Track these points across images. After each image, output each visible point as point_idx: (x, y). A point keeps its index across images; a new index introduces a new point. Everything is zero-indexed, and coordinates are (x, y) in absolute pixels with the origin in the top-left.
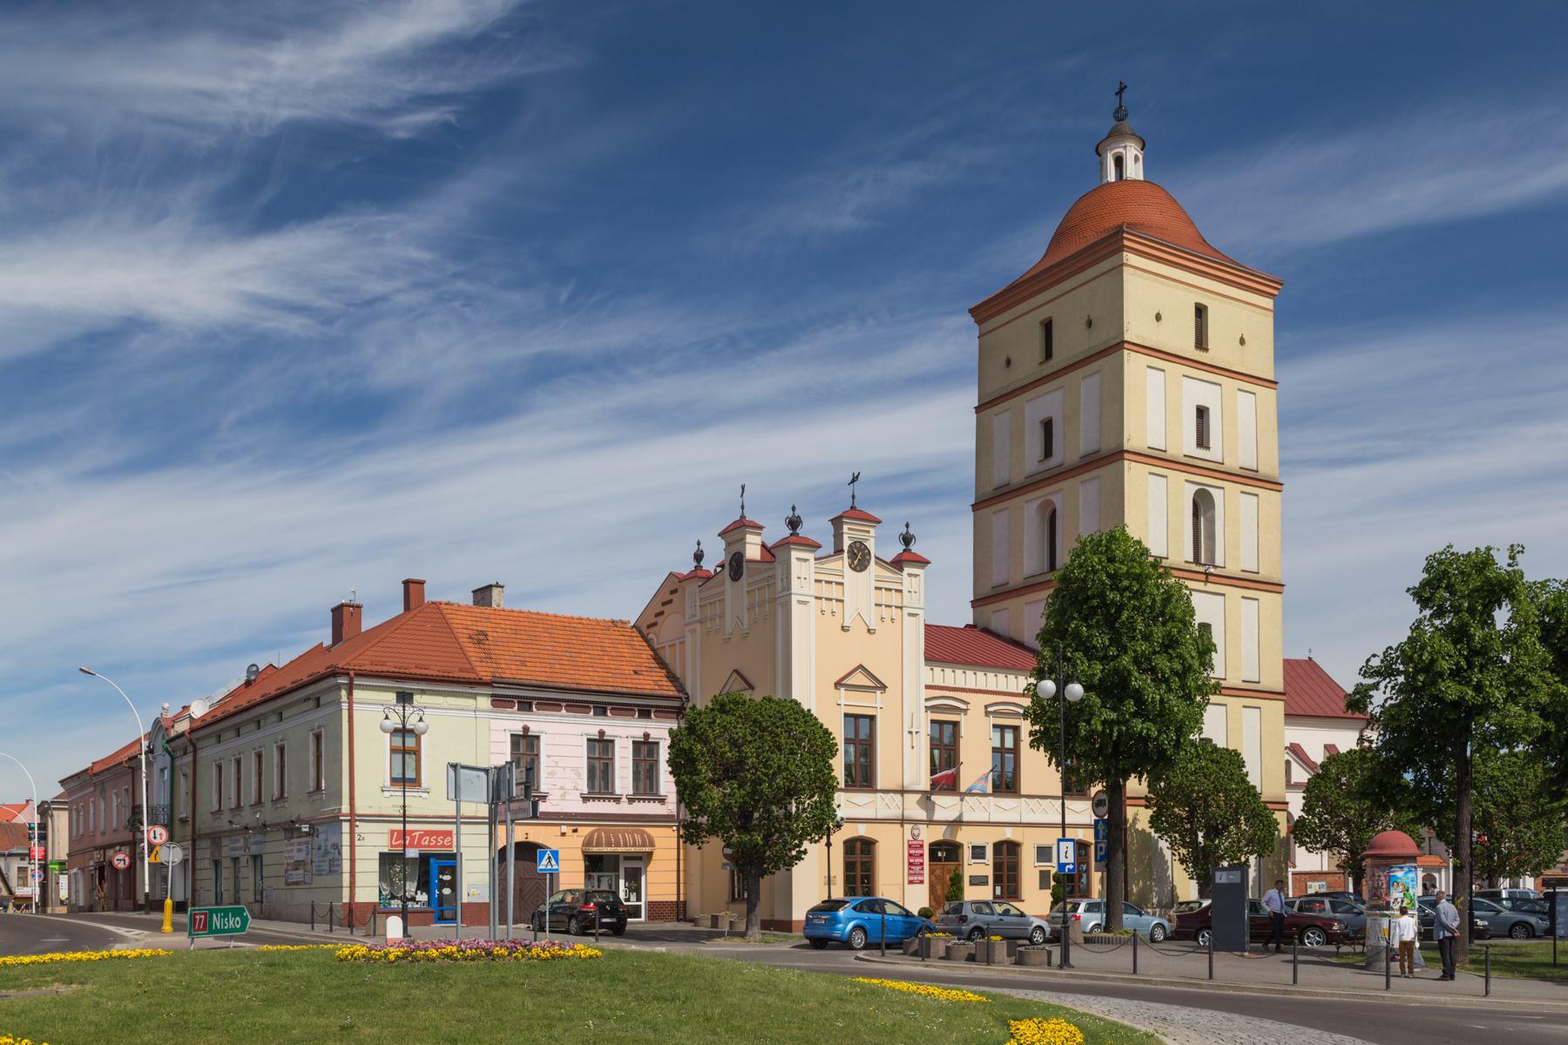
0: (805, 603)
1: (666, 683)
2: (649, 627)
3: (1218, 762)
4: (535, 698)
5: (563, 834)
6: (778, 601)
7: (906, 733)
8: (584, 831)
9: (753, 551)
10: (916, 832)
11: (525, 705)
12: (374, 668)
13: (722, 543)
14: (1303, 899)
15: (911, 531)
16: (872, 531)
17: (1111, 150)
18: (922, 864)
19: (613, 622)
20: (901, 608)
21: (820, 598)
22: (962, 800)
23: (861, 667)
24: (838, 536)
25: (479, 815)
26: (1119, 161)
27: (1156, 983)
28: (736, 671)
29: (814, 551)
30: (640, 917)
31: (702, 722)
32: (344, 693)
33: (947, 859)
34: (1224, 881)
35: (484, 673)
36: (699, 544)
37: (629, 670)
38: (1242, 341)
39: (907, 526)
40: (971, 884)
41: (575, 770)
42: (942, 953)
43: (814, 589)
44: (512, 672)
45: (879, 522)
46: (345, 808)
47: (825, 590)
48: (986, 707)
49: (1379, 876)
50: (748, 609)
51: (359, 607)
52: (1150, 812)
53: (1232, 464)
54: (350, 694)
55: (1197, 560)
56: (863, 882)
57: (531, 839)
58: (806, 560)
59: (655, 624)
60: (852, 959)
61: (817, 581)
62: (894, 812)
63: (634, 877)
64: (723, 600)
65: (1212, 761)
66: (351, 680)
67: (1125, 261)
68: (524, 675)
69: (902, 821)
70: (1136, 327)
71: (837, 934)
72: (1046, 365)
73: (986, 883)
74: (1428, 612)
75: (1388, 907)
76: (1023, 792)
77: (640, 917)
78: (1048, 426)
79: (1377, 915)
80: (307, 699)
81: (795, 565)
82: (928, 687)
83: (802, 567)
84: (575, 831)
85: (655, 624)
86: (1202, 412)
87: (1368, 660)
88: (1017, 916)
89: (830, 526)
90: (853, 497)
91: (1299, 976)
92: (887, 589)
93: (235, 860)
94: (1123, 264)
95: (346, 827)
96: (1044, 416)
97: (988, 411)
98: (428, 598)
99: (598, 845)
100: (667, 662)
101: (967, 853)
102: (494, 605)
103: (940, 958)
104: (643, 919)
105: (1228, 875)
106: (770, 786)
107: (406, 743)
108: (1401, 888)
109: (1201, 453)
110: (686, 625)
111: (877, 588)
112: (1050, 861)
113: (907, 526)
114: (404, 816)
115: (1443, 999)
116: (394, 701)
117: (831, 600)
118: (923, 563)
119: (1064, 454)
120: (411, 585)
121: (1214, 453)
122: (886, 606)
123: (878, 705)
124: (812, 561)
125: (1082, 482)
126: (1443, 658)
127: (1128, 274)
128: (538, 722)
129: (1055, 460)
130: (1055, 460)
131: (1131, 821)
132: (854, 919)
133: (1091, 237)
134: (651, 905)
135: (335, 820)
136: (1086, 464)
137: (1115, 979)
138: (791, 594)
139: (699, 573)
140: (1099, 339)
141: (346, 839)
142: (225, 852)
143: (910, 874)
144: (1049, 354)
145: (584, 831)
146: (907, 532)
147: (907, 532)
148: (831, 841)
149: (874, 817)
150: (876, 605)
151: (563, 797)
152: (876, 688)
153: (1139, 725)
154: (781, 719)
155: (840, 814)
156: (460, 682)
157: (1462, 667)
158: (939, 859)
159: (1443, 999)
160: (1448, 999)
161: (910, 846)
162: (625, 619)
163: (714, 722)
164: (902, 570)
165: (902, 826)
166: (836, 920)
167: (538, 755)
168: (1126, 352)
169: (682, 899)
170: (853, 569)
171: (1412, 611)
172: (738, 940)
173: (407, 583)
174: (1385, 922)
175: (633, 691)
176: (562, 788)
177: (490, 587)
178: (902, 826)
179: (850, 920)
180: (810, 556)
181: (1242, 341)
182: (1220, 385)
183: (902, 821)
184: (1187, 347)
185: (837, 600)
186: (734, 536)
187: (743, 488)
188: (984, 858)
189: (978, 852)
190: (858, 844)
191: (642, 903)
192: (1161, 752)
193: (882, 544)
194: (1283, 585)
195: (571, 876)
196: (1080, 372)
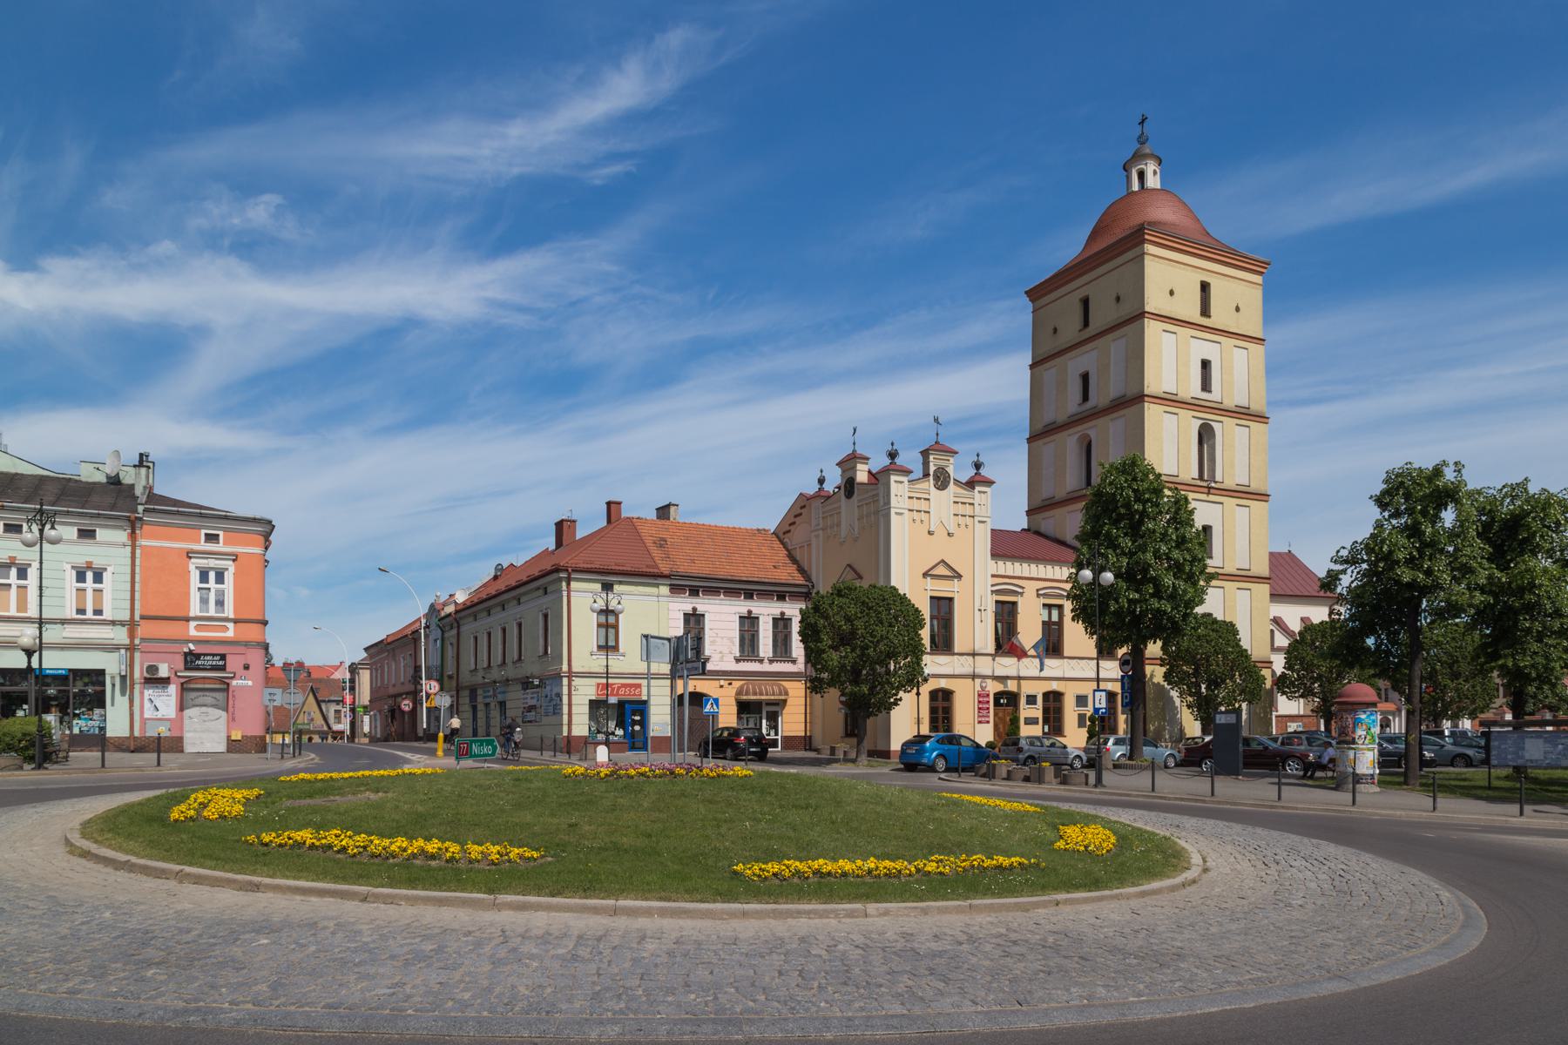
0: (901, 514)
1: (797, 574)
2: (784, 533)
3: (1217, 631)
4: (701, 587)
5: (722, 686)
6: (881, 513)
7: (977, 612)
8: (737, 684)
9: (862, 476)
10: (984, 685)
11: (694, 592)
12: (586, 566)
13: (839, 471)
14: (1285, 736)
15: (981, 459)
16: (952, 460)
17: (1136, 166)
18: (988, 708)
19: (758, 530)
20: (973, 517)
21: (912, 510)
23: (943, 561)
24: (926, 464)
25: (661, 672)
26: (1141, 175)
27: (1170, 799)
28: (849, 565)
29: (907, 476)
30: (777, 747)
31: (824, 603)
32: (564, 584)
33: (1007, 705)
34: (1223, 721)
35: (664, 568)
36: (821, 471)
37: (769, 565)
38: (1238, 309)
39: (978, 455)
40: (1026, 724)
41: (731, 639)
42: (1005, 775)
43: (907, 504)
44: (684, 568)
45: (957, 453)
46: (565, 667)
47: (916, 505)
48: (1038, 590)
49: (1347, 718)
50: (858, 519)
51: (574, 521)
52: (1164, 669)
53: (1229, 403)
54: (568, 585)
55: (1201, 477)
56: (944, 722)
57: (698, 690)
58: (901, 482)
59: (789, 531)
60: (936, 779)
61: (910, 498)
62: (968, 670)
63: (773, 719)
64: (840, 513)
65: (1213, 630)
66: (569, 574)
67: (1146, 251)
68: (694, 570)
69: (974, 677)
70: (1155, 300)
71: (925, 761)
72: (1082, 333)
73: (1037, 723)
74: (1386, 514)
75: (1353, 742)
76: (1065, 655)
77: (777, 747)
78: (1085, 378)
79: (1345, 748)
80: (538, 588)
81: (893, 486)
82: (993, 576)
83: (899, 489)
84: (730, 684)
85: (789, 531)
86: (1206, 365)
87: (1338, 552)
88: (1061, 747)
89: (920, 458)
90: (937, 434)
91: (1283, 795)
92: (962, 503)
93: (487, 705)
94: (1144, 253)
95: (565, 681)
96: (1082, 370)
97: (1039, 367)
98: (624, 514)
99: (747, 694)
100: (798, 559)
101: (1023, 700)
102: (671, 519)
103: (1004, 779)
104: (779, 749)
105: (1226, 718)
106: (875, 651)
107: (608, 620)
108: (1364, 727)
109: (1205, 395)
110: (812, 532)
111: (955, 502)
112: (1086, 706)
113: (978, 455)
114: (607, 673)
115: (1398, 813)
116: (600, 590)
117: (920, 511)
118: (989, 483)
119: (1098, 399)
120: (612, 505)
121: (1215, 395)
122: (962, 515)
123: (956, 590)
124: (906, 482)
125: (1112, 420)
126: (1399, 550)
127: (1148, 260)
128: (704, 605)
129: (1090, 404)
130: (1090, 404)
131: (1149, 676)
132: (938, 749)
133: (1118, 233)
134: (785, 738)
135: (558, 677)
136: (1116, 406)
137: (1138, 796)
138: (890, 508)
139: (823, 493)
140: (1126, 310)
141: (565, 690)
142: (480, 699)
143: (979, 716)
144: (1086, 324)
145: (737, 684)
146: (978, 460)
147: (978, 460)
148: (920, 691)
150: (955, 515)
151: (721, 659)
152: (954, 577)
153: (1154, 603)
154: (883, 601)
155: (927, 671)
156: (647, 576)
157: (1414, 556)
158: (1002, 705)
159: (1398, 813)
160: (1403, 813)
161: (979, 695)
162: (767, 528)
163: (833, 603)
164: (974, 488)
165: (973, 679)
166: (924, 750)
167: (703, 628)
168: (1146, 320)
169: (808, 734)
170: (938, 489)
171: (1375, 513)
172: (850, 765)
173: (609, 504)
174: (1351, 753)
175: (773, 581)
176: (721, 653)
177: (668, 506)
178: (973, 679)
179: (934, 750)
180: (905, 479)
181: (1238, 309)
182: (1220, 343)
183: (974, 677)
184: (1193, 314)
185: (925, 512)
186: (848, 465)
187: (855, 430)
188: (1035, 704)
189: (1031, 700)
191: (779, 737)
192: (1174, 623)
193: (959, 469)
194: (1269, 495)
195: (728, 717)
196: (1110, 336)
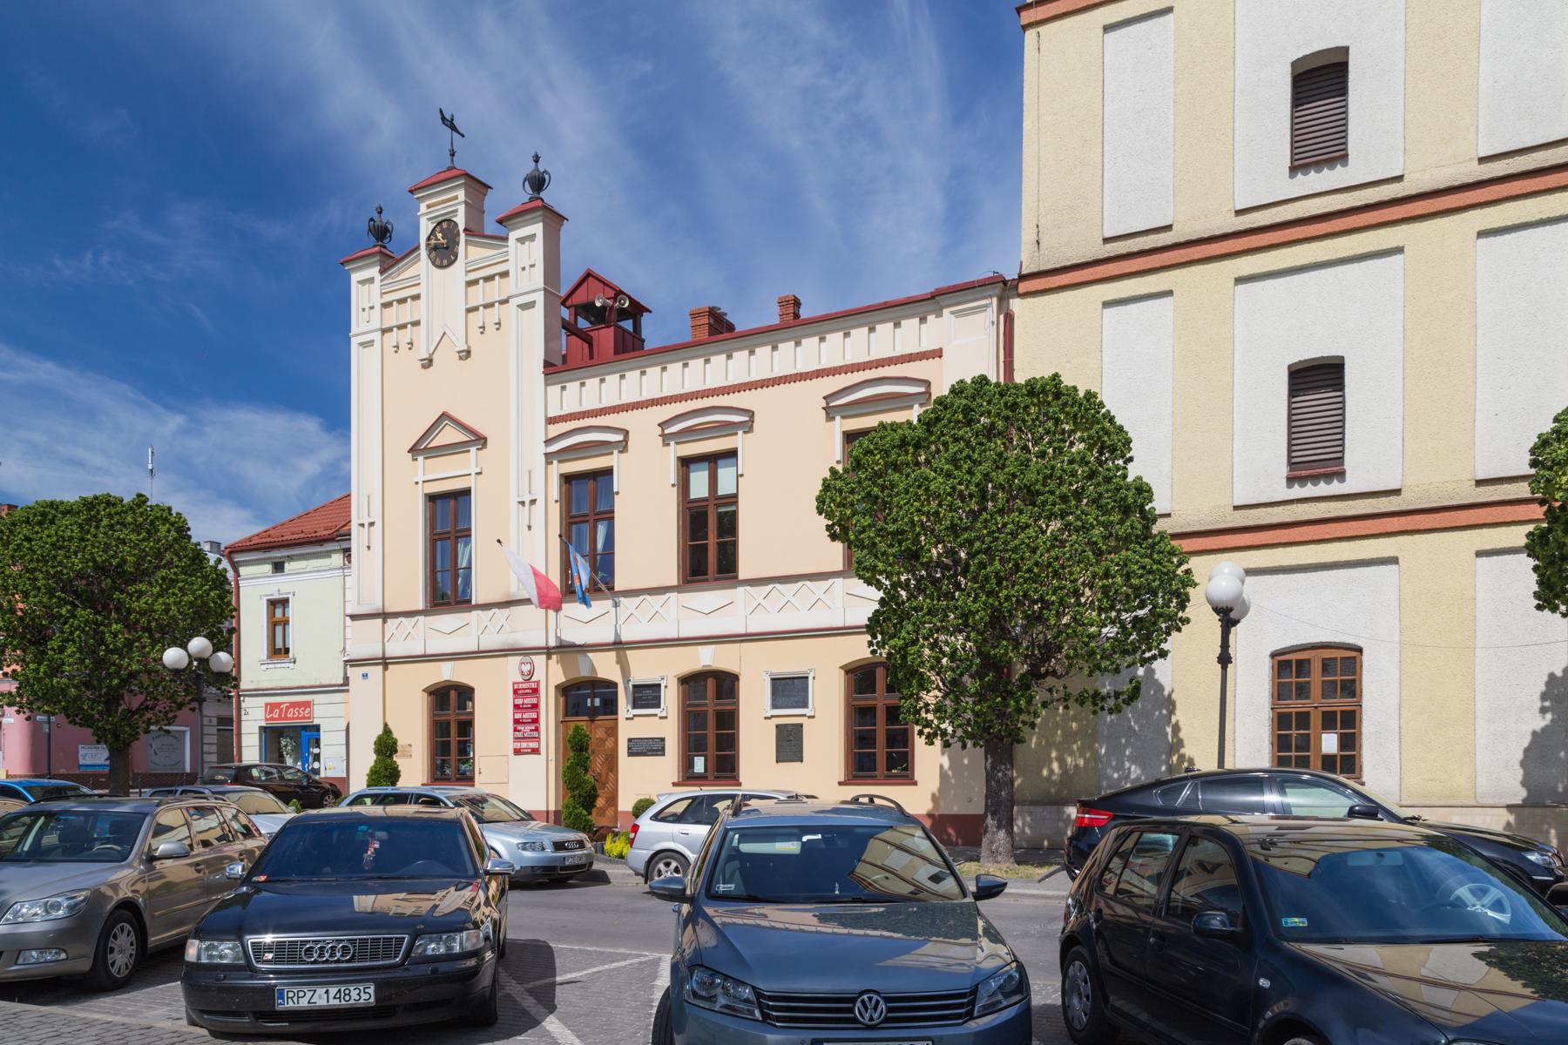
22: (616, 605)
40: (631, 754)
73: (660, 751)
82: (551, 421)
143: (516, 739)
146: (537, 169)
149: (676, 636)
161: (515, 691)
188: (874, 692)
189: (647, 696)
190: (453, 694)
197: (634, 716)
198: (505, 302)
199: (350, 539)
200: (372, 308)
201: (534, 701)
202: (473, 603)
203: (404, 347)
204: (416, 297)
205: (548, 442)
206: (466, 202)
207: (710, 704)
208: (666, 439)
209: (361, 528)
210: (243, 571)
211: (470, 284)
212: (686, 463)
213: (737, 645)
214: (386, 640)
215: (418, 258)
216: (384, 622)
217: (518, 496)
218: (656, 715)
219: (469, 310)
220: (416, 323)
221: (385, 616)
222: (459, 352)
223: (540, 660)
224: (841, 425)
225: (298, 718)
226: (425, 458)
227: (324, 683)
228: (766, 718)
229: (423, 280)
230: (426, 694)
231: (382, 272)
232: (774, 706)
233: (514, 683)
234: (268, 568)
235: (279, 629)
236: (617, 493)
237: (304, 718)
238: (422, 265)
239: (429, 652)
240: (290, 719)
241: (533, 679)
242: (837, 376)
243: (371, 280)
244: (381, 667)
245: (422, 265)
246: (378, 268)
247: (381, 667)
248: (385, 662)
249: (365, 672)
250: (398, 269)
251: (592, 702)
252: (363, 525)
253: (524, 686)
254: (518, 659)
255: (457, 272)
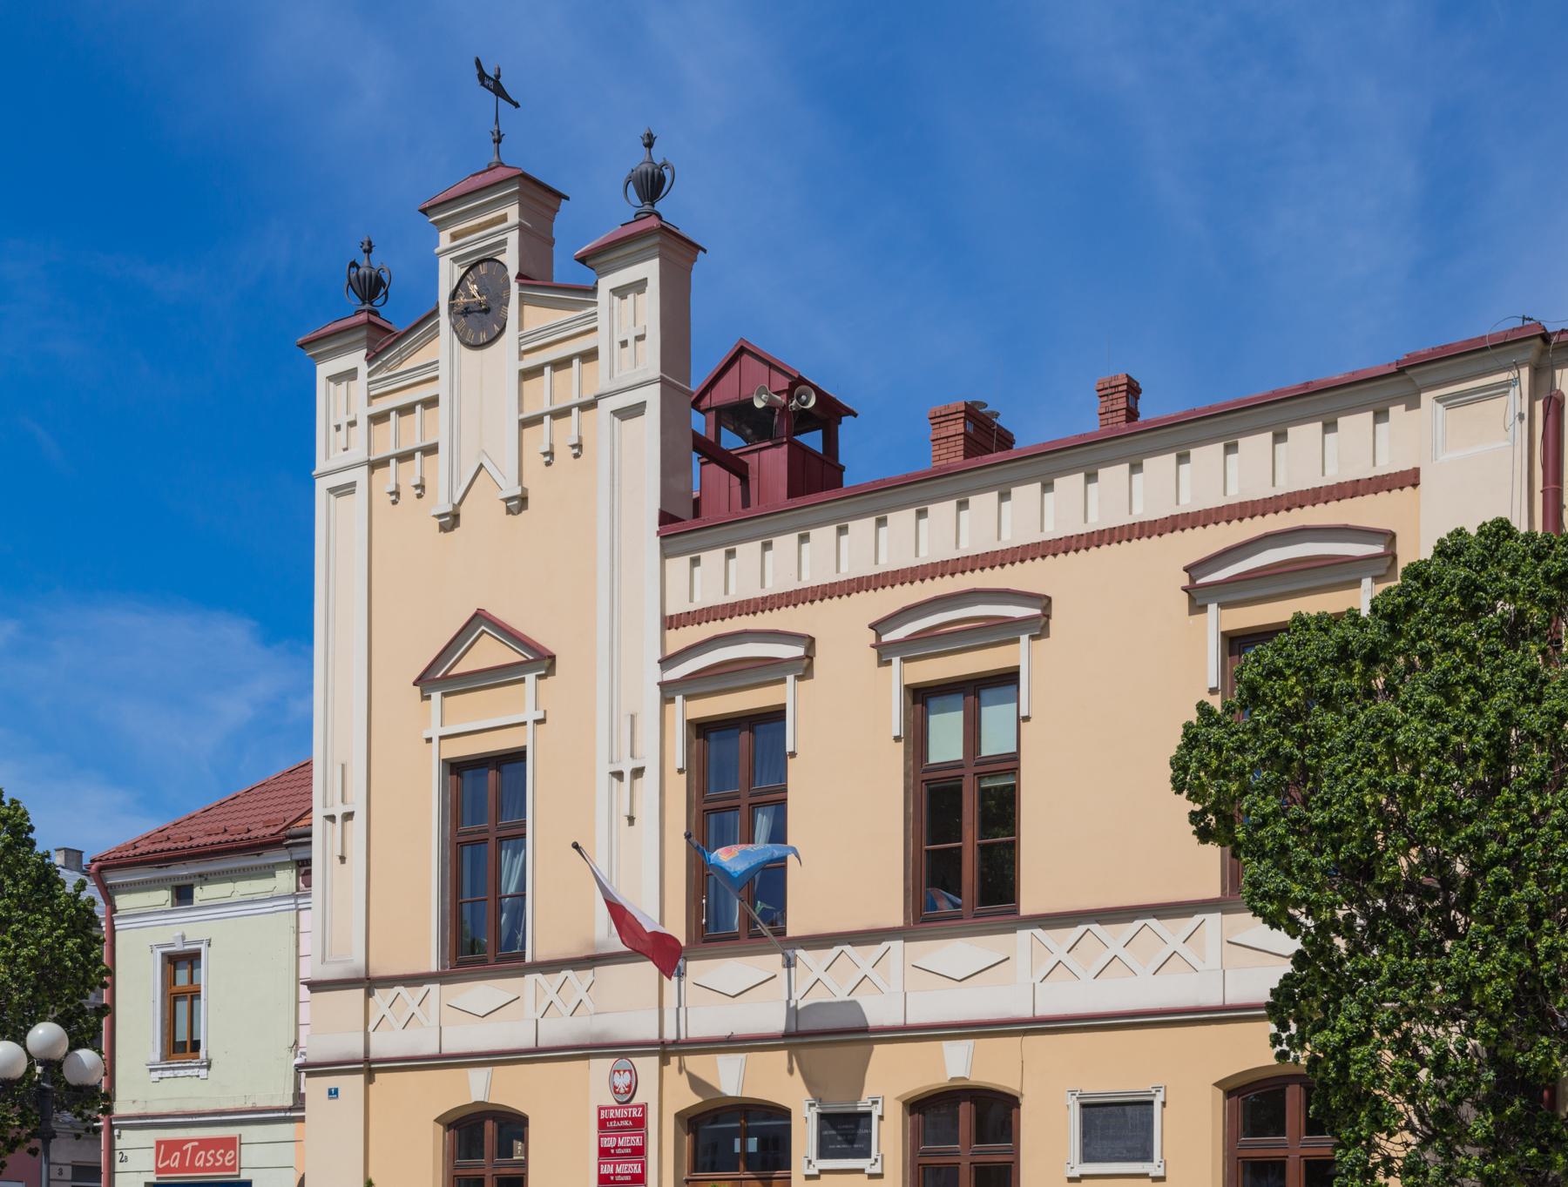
22: (789, 964)
161: (603, 1124)
190: (490, 1127)
197: (822, 1171)
198: (590, 405)
199: (310, 843)
200: (352, 424)
201: (637, 1141)
202: (528, 959)
203: (408, 493)
204: (431, 402)
205: (667, 662)
206: (521, 226)
207: (965, 1152)
208: (884, 653)
209: (329, 823)
210: (122, 901)
211: (527, 374)
212: (921, 697)
213: (1017, 1040)
214: (371, 1028)
215: (434, 332)
216: (369, 994)
217: (611, 762)
218: (862, 1171)
219: (525, 423)
220: (431, 450)
221: (369, 983)
222: (507, 500)
223: (647, 1066)
224: (1216, 621)
225: (213, 1168)
226: (445, 695)
227: (261, 1104)
228: (1071, 1180)
229: (443, 372)
230: (440, 1128)
231: (370, 359)
232: (1087, 1157)
233: (600, 1109)
234: (163, 897)
235: (183, 1007)
236: (793, 754)
237: (223, 1168)
238: (443, 345)
239: (448, 1048)
240: (199, 1169)
241: (634, 1102)
242: (1211, 527)
243: (351, 374)
244: (361, 1078)
245: (443, 345)
246: (364, 351)
247: (361, 1078)
248: (369, 1067)
249: (333, 1086)
250: (401, 352)
251: (744, 1145)
252: (332, 818)
253: (618, 1114)
254: (608, 1063)
255: (505, 354)
